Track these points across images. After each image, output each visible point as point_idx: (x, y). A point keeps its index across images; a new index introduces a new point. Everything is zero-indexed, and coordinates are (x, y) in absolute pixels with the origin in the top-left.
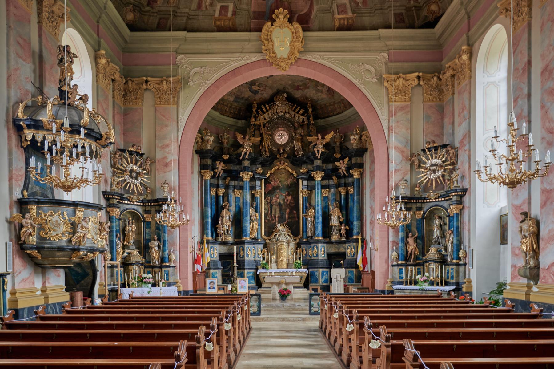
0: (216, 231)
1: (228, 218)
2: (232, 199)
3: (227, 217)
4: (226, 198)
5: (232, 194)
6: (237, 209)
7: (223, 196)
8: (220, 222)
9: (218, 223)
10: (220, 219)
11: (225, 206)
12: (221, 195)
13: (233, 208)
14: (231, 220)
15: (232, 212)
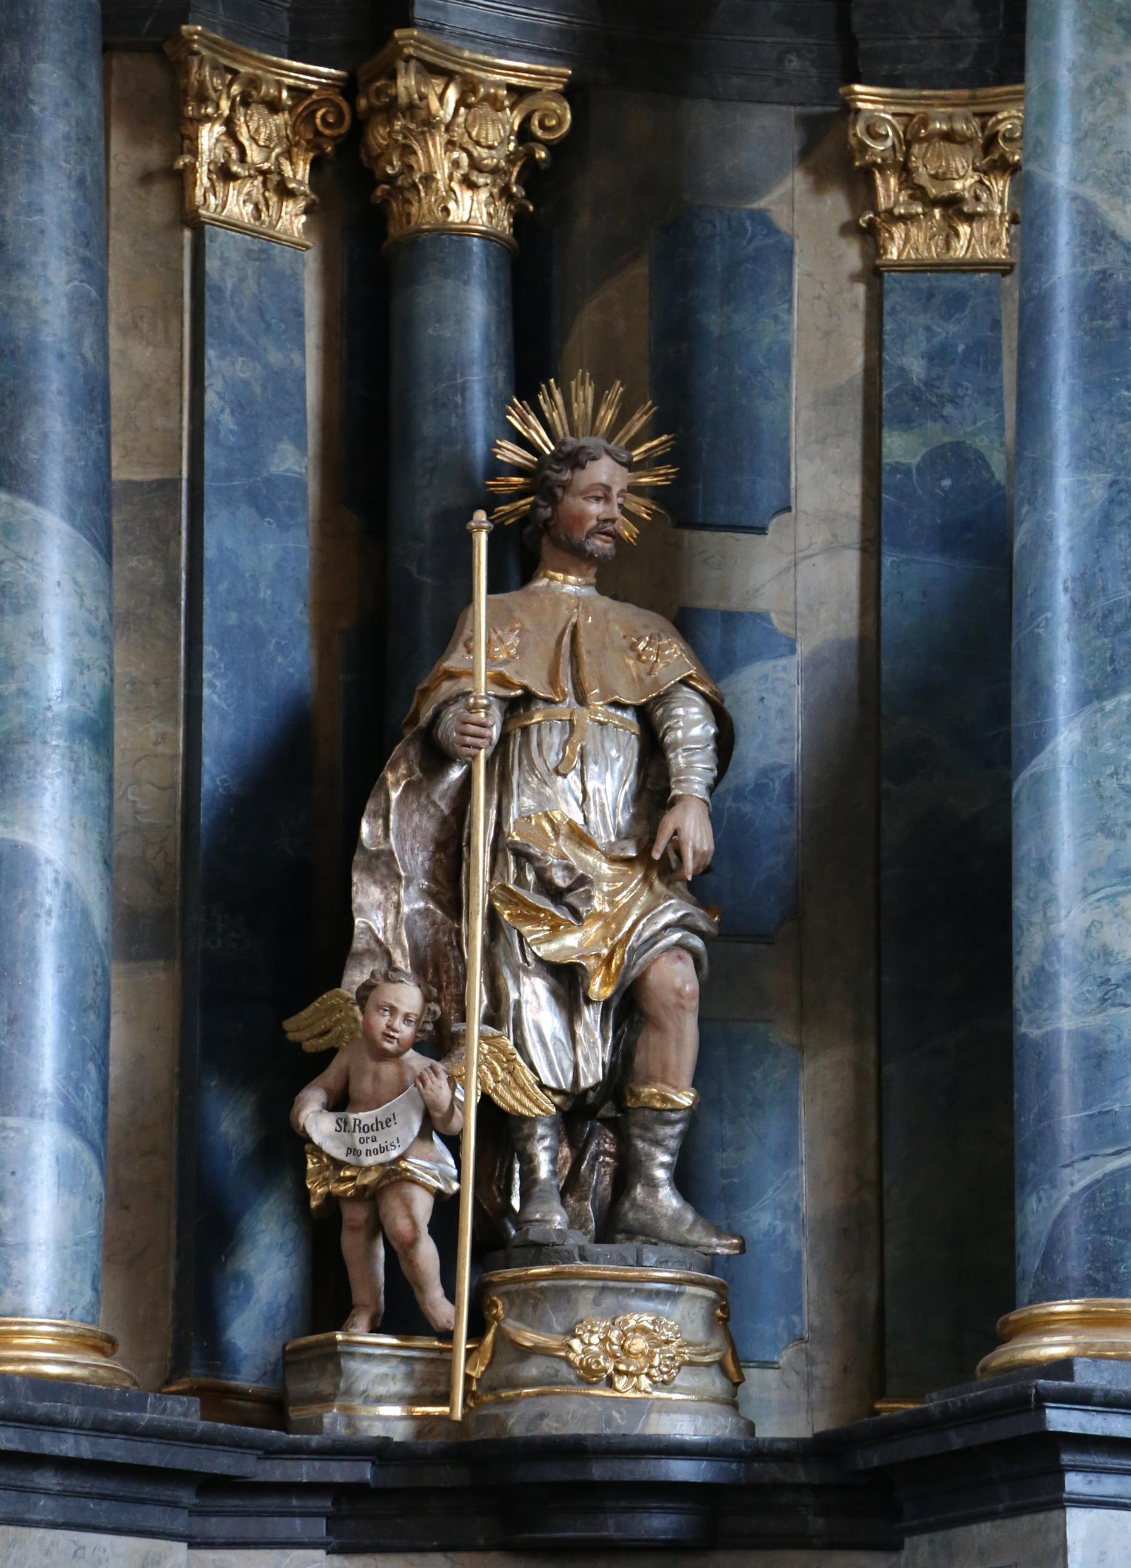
0: (286, 1148)
1: (605, 788)
2: (810, 336)
3: (581, 784)
4: (608, 310)
5: (802, 212)
6: (918, 575)
7: (533, 270)
8: (383, 912)
9: (330, 936)
10: (395, 825)
11: (545, 478)
12: (471, 209)
13: (802, 575)
14: (693, 829)
15: (781, 707)
